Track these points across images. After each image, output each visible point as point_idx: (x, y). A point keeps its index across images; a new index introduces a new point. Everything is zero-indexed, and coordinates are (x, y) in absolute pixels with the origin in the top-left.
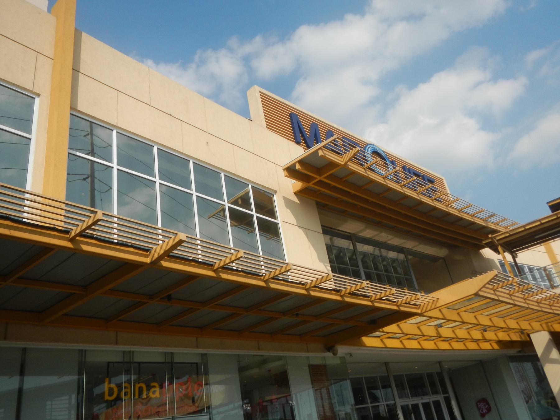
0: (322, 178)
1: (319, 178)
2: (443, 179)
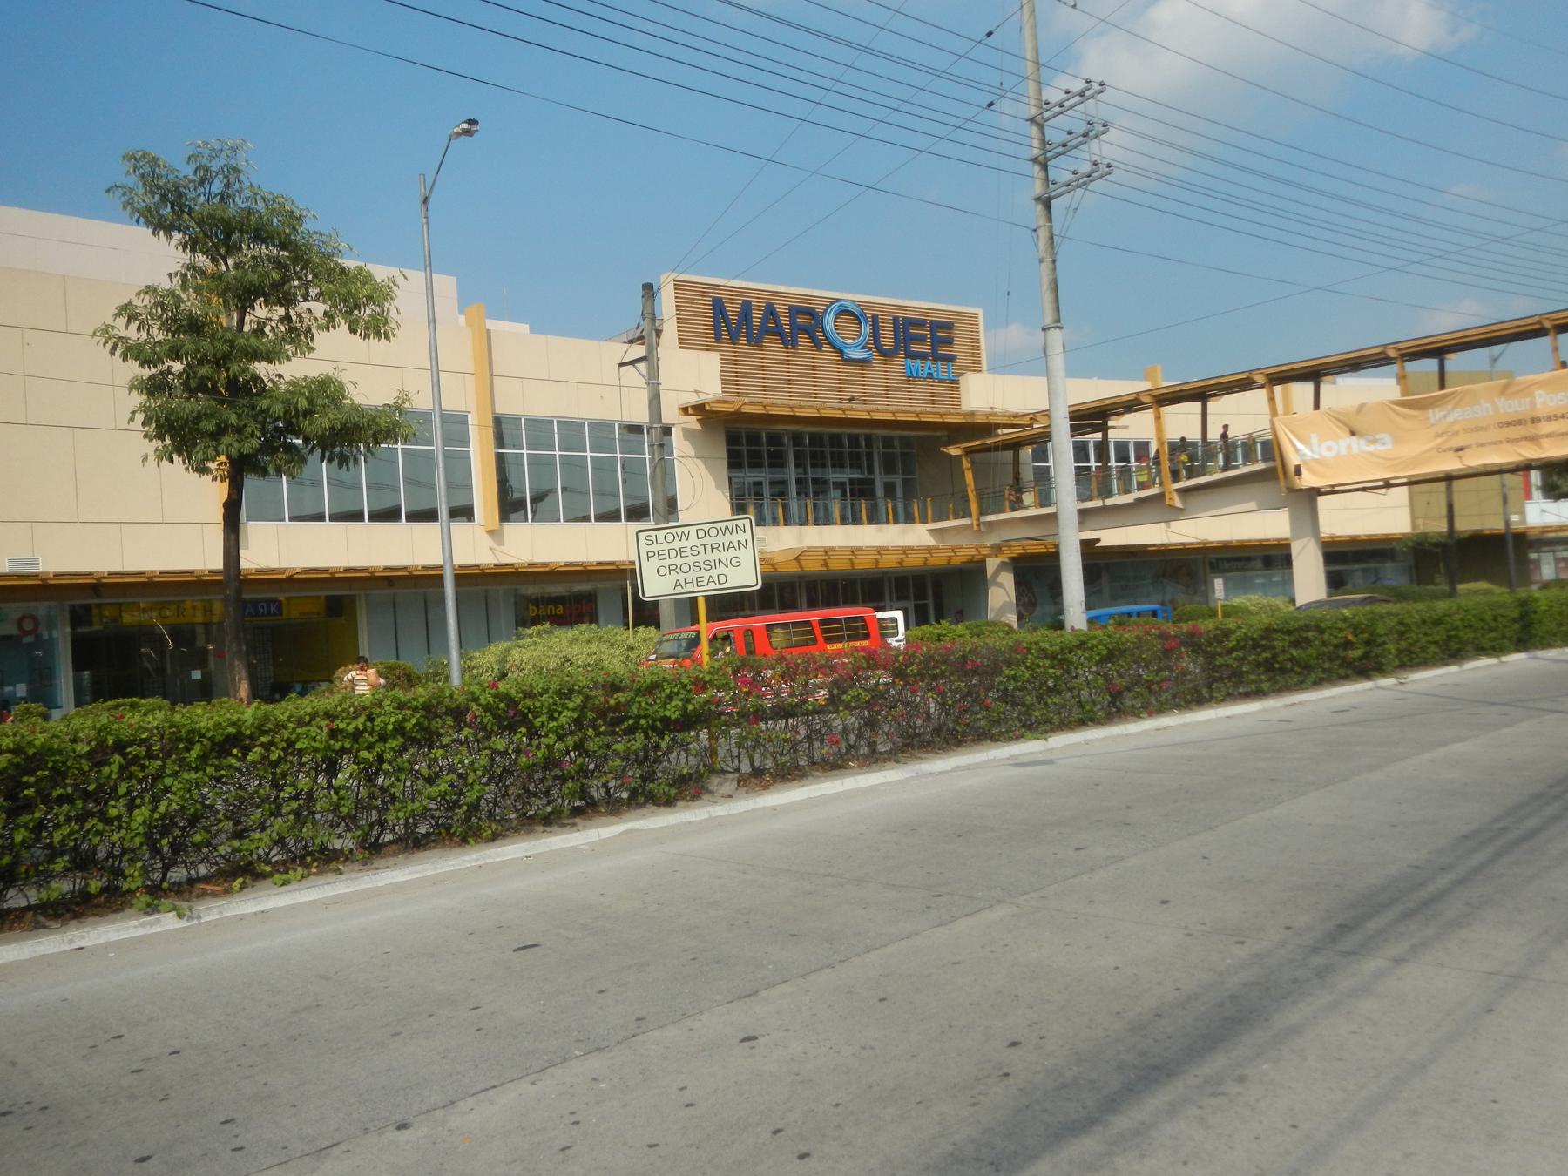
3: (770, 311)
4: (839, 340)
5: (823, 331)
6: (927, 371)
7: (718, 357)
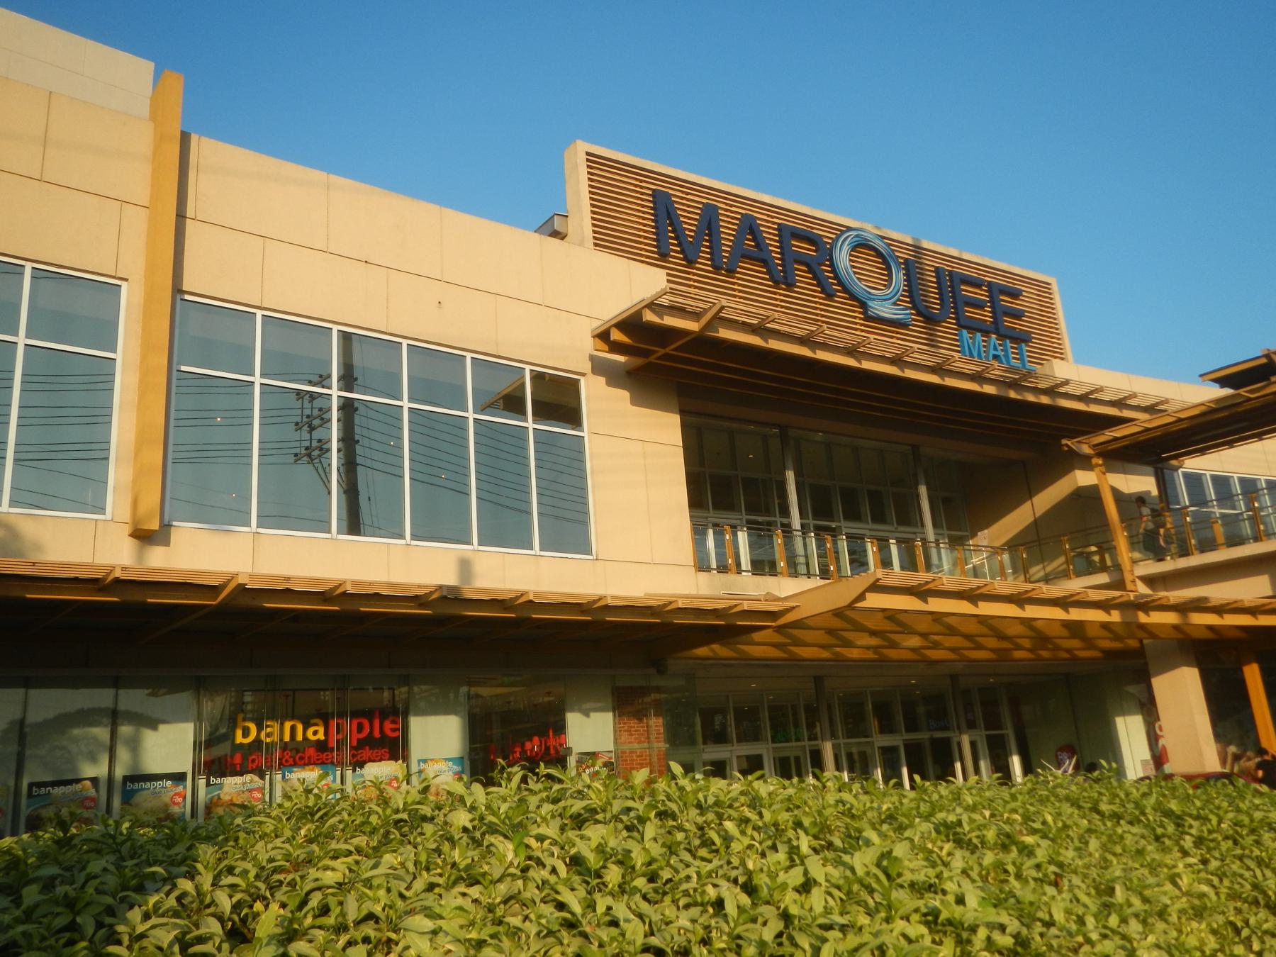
0: (668, 350)
1: (661, 351)
2: (1049, 284)
3: (749, 227)
4: (860, 287)
6: (992, 352)
7: (666, 278)
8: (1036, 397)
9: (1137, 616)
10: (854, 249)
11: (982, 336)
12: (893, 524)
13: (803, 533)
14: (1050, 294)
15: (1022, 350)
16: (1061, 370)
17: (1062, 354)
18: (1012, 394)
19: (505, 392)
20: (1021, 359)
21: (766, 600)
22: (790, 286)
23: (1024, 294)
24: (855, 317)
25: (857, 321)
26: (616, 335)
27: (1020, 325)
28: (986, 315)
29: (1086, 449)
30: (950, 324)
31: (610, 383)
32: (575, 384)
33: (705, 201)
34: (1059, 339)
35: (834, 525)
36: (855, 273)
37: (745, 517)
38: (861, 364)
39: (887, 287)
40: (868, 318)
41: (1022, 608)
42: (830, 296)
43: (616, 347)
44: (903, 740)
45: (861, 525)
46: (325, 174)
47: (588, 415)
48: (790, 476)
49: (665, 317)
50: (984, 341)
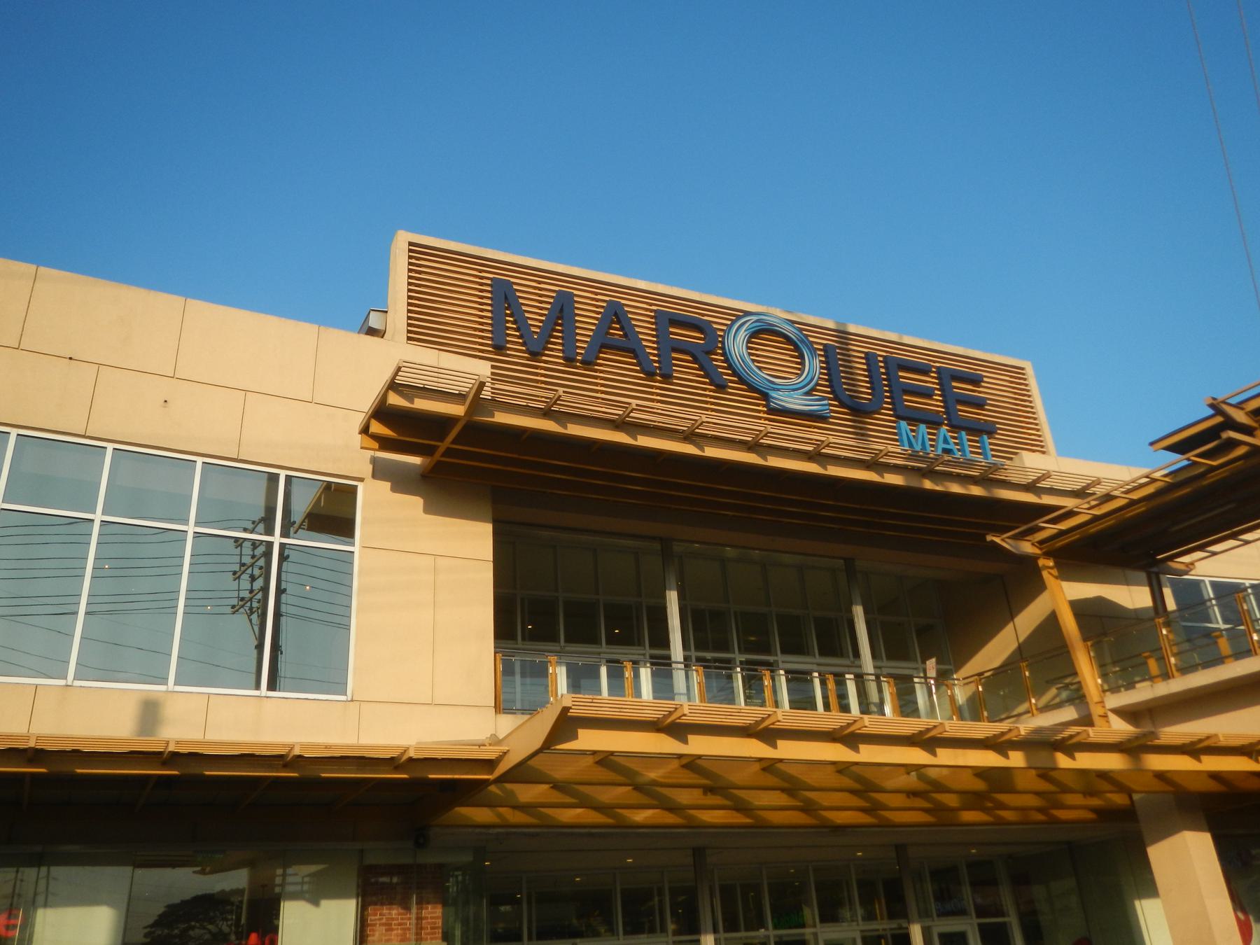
2: (1023, 369)
4: (761, 377)
5: (724, 354)
6: (941, 445)
8: (943, 485)
9: (1054, 760)
10: (755, 334)
11: (928, 428)
12: (849, 657)
13: (686, 666)
14: (1025, 379)
15: (983, 443)
16: (1031, 463)
17: (1042, 447)
18: (928, 485)
19: (307, 512)
20: (984, 454)
21: (490, 745)
22: (667, 378)
23: (985, 379)
24: (759, 411)
25: (761, 415)
26: (376, 428)
27: (983, 416)
28: (935, 404)
29: (1027, 547)
30: (885, 416)
31: (394, 489)
32: (353, 491)
33: (607, 298)
34: (1038, 430)
35: (771, 659)
36: (753, 361)
37: (649, 651)
38: (704, 452)
39: (799, 375)
40: (772, 411)
41: (856, 750)
42: (721, 387)
43: (385, 444)
44: (862, 931)
45: (808, 659)
46: (34, 267)
47: (363, 523)
48: (672, 598)
49: (416, 400)
50: (929, 434)
